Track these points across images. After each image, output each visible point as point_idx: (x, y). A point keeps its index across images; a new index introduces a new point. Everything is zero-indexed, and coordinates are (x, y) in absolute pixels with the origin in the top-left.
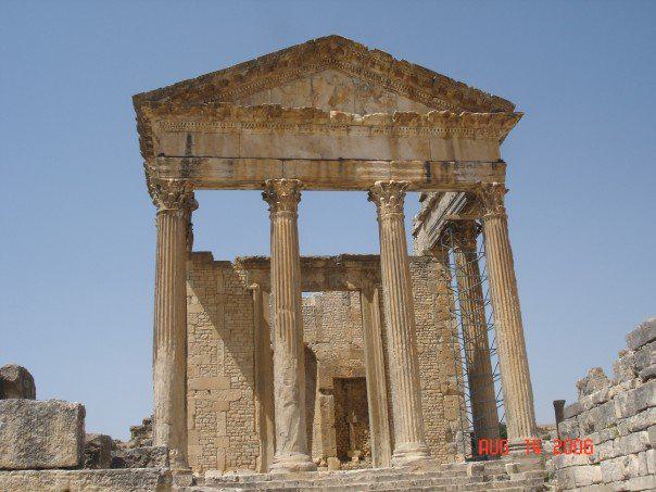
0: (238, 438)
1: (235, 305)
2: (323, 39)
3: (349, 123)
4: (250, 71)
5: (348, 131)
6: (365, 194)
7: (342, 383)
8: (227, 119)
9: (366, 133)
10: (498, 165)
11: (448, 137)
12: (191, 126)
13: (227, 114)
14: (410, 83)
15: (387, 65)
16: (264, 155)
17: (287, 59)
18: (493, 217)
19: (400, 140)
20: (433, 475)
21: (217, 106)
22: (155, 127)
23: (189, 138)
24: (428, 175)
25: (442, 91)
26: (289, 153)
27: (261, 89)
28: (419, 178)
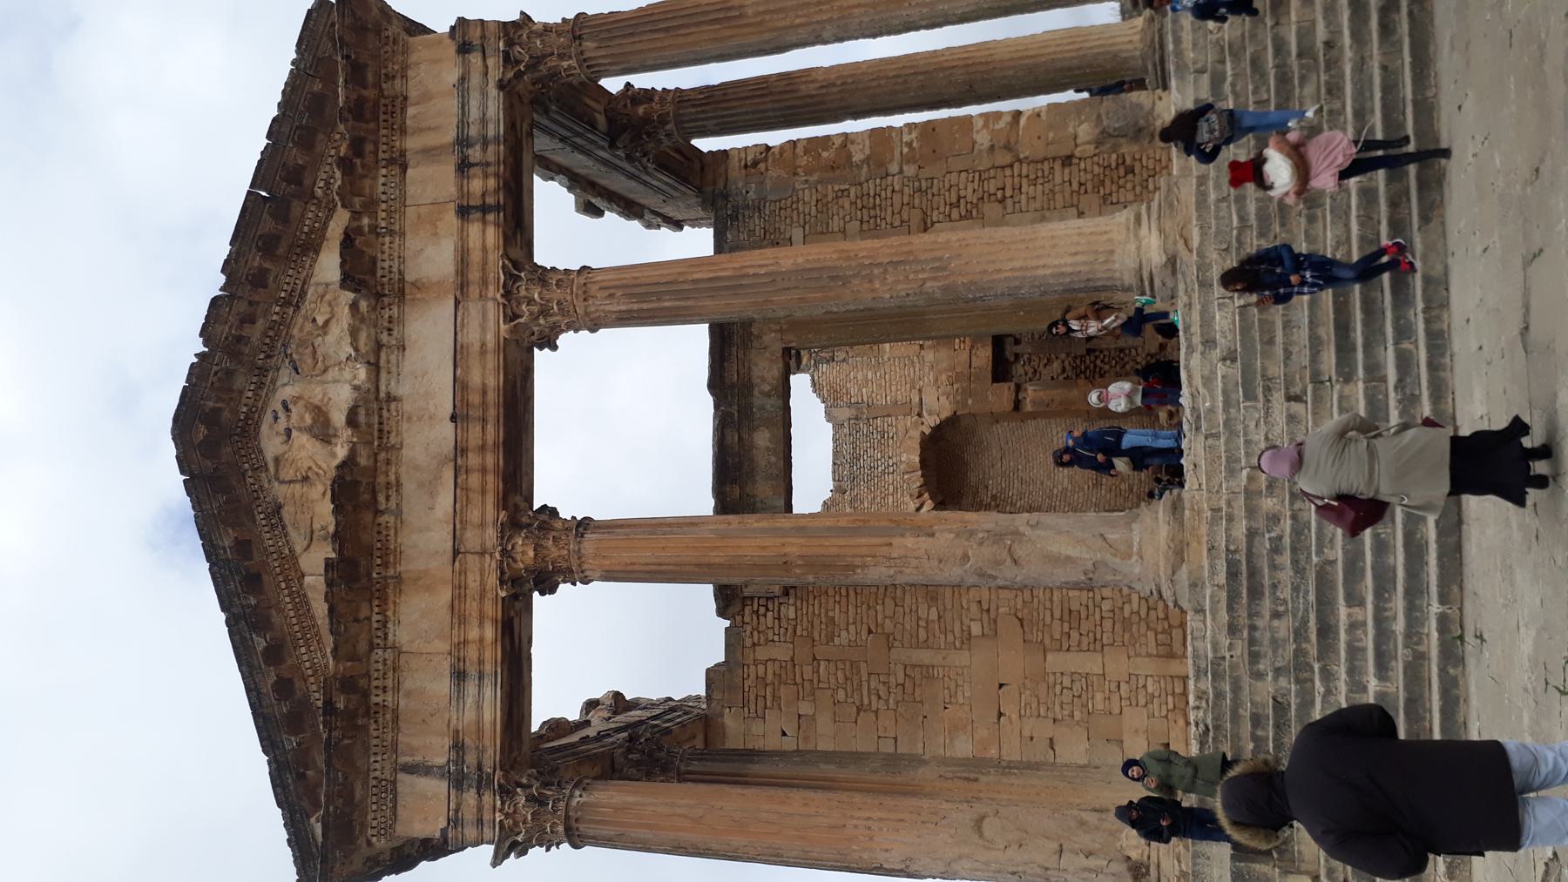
0: (1108, 624)
1: (816, 621)
3: (372, 397)
5: (391, 398)
7: (1001, 370)
8: (363, 682)
10: (466, 35)
14: (281, 251)
16: (446, 595)
17: (226, 544)
20: (1201, 202)
22: (380, 844)
23: (411, 769)
24: (484, 209)
25: (295, 176)
27: (301, 601)
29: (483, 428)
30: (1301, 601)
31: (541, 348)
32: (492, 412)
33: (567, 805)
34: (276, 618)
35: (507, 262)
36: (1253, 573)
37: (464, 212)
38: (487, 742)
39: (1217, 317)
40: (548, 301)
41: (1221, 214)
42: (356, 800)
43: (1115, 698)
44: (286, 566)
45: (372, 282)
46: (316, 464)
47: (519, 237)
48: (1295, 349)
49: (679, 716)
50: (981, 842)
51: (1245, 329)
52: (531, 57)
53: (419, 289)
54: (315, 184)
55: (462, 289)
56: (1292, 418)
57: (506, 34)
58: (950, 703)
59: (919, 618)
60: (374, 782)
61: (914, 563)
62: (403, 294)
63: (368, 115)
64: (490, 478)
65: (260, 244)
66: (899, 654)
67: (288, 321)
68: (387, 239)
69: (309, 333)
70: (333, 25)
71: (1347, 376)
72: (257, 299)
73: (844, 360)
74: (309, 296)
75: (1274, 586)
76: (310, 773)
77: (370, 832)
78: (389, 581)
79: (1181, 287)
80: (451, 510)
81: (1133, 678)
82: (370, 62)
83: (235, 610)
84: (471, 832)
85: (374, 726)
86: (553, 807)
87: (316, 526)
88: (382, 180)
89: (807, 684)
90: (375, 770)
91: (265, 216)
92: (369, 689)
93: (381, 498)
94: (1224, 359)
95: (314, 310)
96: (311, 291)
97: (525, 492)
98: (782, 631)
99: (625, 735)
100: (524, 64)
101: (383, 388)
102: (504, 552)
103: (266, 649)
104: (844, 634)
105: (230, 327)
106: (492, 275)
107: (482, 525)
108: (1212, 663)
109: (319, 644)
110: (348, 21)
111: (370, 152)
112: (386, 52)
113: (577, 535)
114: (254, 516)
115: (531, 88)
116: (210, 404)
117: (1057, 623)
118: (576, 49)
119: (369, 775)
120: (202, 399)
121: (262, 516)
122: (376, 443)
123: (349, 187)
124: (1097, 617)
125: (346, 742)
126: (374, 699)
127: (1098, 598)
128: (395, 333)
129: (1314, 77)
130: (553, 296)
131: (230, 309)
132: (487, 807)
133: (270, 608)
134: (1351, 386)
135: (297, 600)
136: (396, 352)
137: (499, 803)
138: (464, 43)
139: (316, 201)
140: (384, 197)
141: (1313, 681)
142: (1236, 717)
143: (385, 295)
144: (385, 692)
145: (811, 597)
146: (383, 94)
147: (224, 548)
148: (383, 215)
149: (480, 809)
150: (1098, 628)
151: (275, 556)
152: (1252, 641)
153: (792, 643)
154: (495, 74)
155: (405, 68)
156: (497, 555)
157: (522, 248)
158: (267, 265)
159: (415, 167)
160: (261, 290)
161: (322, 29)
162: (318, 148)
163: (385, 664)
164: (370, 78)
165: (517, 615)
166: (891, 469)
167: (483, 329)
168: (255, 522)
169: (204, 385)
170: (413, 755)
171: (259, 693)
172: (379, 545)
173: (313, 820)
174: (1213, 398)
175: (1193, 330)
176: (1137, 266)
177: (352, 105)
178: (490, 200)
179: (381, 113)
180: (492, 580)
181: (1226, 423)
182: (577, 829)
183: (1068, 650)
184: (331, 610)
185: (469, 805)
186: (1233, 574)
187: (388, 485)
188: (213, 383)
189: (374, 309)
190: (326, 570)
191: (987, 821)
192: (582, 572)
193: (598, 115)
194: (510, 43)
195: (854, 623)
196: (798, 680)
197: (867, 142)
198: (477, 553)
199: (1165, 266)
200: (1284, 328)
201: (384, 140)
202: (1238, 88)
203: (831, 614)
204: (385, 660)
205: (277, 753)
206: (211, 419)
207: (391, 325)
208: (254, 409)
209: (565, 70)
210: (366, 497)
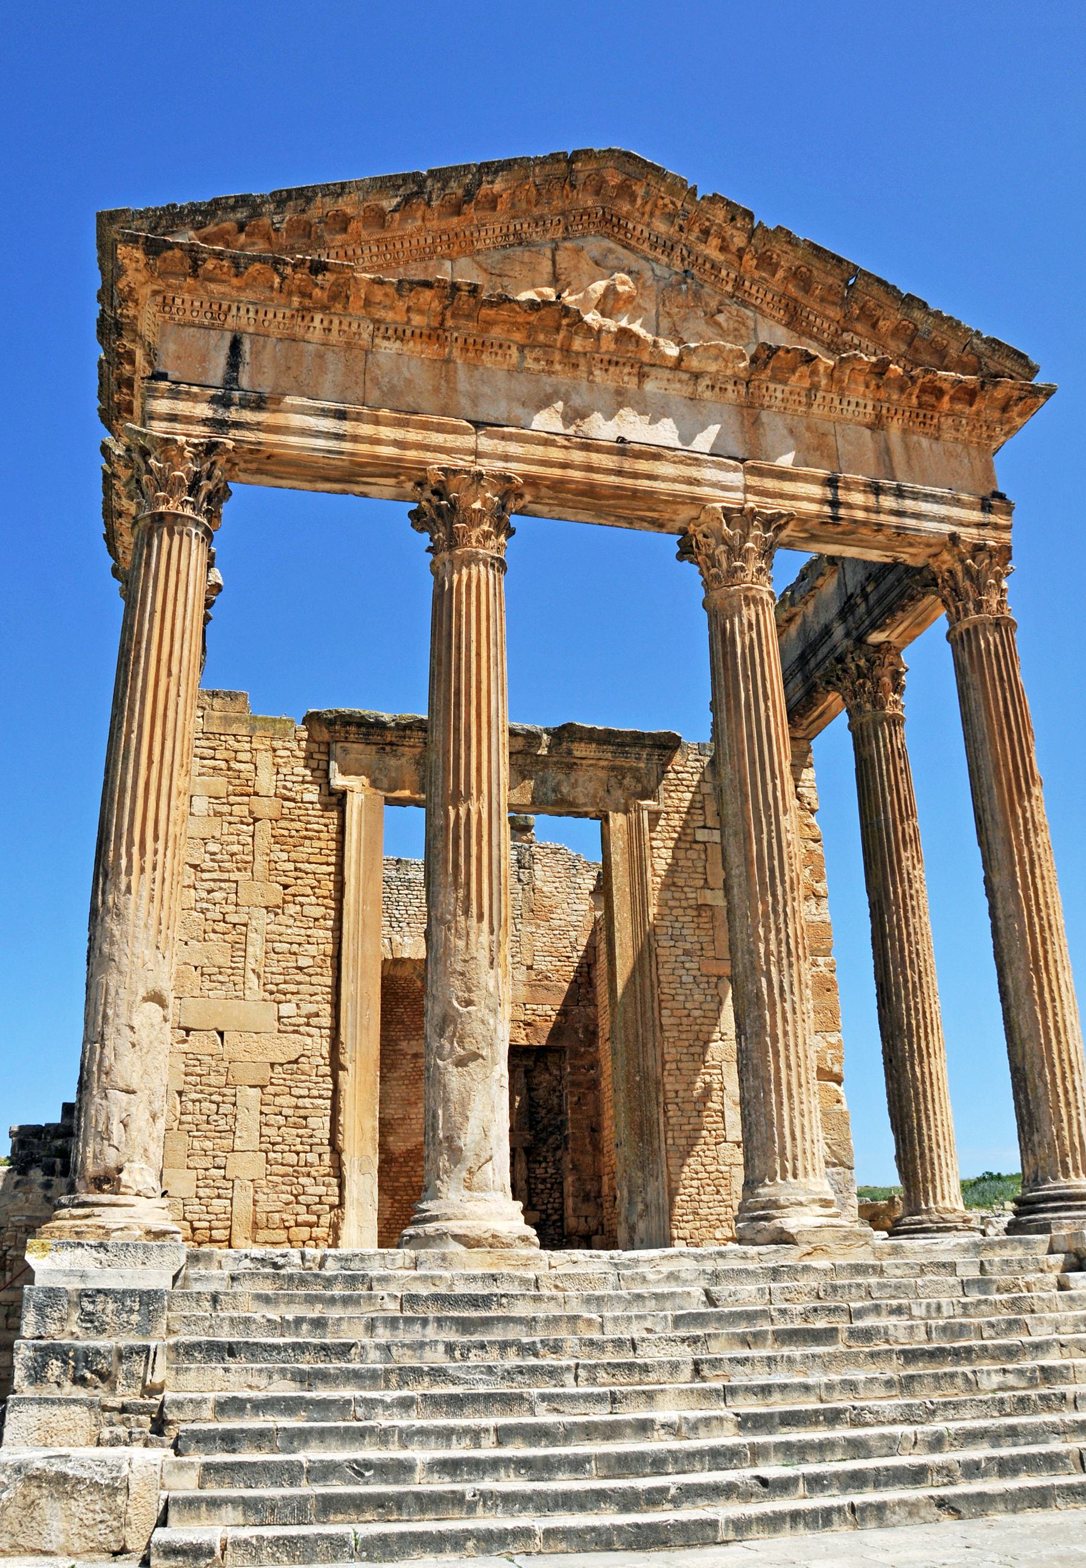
0: (292, 1158)
1: (298, 825)
2: (587, 154)
3: (646, 358)
4: (407, 200)
5: (642, 376)
6: (671, 543)
8: (338, 307)
12: (243, 320)
14: (792, 289)
15: (739, 240)
17: (498, 187)
19: (765, 416)
20: (859, 1269)
21: (318, 268)
23: (235, 346)
24: (835, 504)
27: (426, 255)
28: (814, 508)
30: (477, 1377)
31: (679, 542)
32: (628, 482)
34: (410, 227)
36: (487, 1322)
37: (831, 483)
39: (749, 1288)
41: (853, 1290)
43: (207, 1162)
45: (763, 377)
47: (802, 535)
48: (747, 1369)
50: (139, 998)
51: (750, 1317)
52: (978, 571)
54: (856, 333)
56: (675, 1367)
58: (202, 974)
59: (300, 944)
60: (225, 307)
61: (461, 944)
63: (925, 398)
64: (557, 472)
65: (803, 269)
66: (261, 920)
68: (804, 400)
69: (707, 305)
70: (1011, 377)
71: (747, 1423)
72: (746, 257)
73: (520, 880)
75: (482, 1346)
79: (763, 1249)
81: (229, 1184)
82: (974, 408)
83: (429, 182)
85: (288, 313)
86: (187, 502)
87: (506, 281)
89: (226, 809)
90: (238, 309)
91: (830, 280)
93: (538, 352)
94: (707, 1293)
98: (289, 785)
101: (653, 372)
103: (382, 209)
104: (284, 856)
106: (769, 500)
108: (363, 1276)
110: (1016, 394)
117: (293, 1101)
121: (518, 227)
122: (597, 356)
124: (299, 1148)
127: (320, 1149)
128: (708, 394)
129: (1023, 1384)
130: (752, 563)
132: (191, 427)
133: (423, 219)
134: (734, 1430)
136: (690, 389)
137: (196, 441)
138: (990, 506)
140: (845, 403)
141: (387, 1387)
142: (311, 1300)
145: (327, 821)
147: (492, 182)
148: (828, 400)
149: (188, 420)
150: (287, 1148)
151: (476, 235)
152: (409, 1321)
153: (276, 795)
155: (966, 444)
160: (755, 262)
162: (892, 344)
164: (959, 407)
166: (394, 924)
167: (714, 485)
168: (513, 218)
171: (339, 195)
172: (488, 344)
173: (192, 233)
174: (659, 1281)
175: (720, 1261)
176: (782, 1202)
177: (937, 383)
178: (842, 512)
181: (639, 1297)
183: (262, 1113)
186: (484, 1301)
187: (550, 362)
189: (735, 375)
190: (470, 284)
191: (155, 1006)
195: (296, 869)
196: (232, 799)
197: (817, 918)
199: (782, 1231)
200: (769, 1358)
202: (983, 1307)
203: (307, 842)
206: (625, 190)
207: (717, 389)
210: (541, 337)
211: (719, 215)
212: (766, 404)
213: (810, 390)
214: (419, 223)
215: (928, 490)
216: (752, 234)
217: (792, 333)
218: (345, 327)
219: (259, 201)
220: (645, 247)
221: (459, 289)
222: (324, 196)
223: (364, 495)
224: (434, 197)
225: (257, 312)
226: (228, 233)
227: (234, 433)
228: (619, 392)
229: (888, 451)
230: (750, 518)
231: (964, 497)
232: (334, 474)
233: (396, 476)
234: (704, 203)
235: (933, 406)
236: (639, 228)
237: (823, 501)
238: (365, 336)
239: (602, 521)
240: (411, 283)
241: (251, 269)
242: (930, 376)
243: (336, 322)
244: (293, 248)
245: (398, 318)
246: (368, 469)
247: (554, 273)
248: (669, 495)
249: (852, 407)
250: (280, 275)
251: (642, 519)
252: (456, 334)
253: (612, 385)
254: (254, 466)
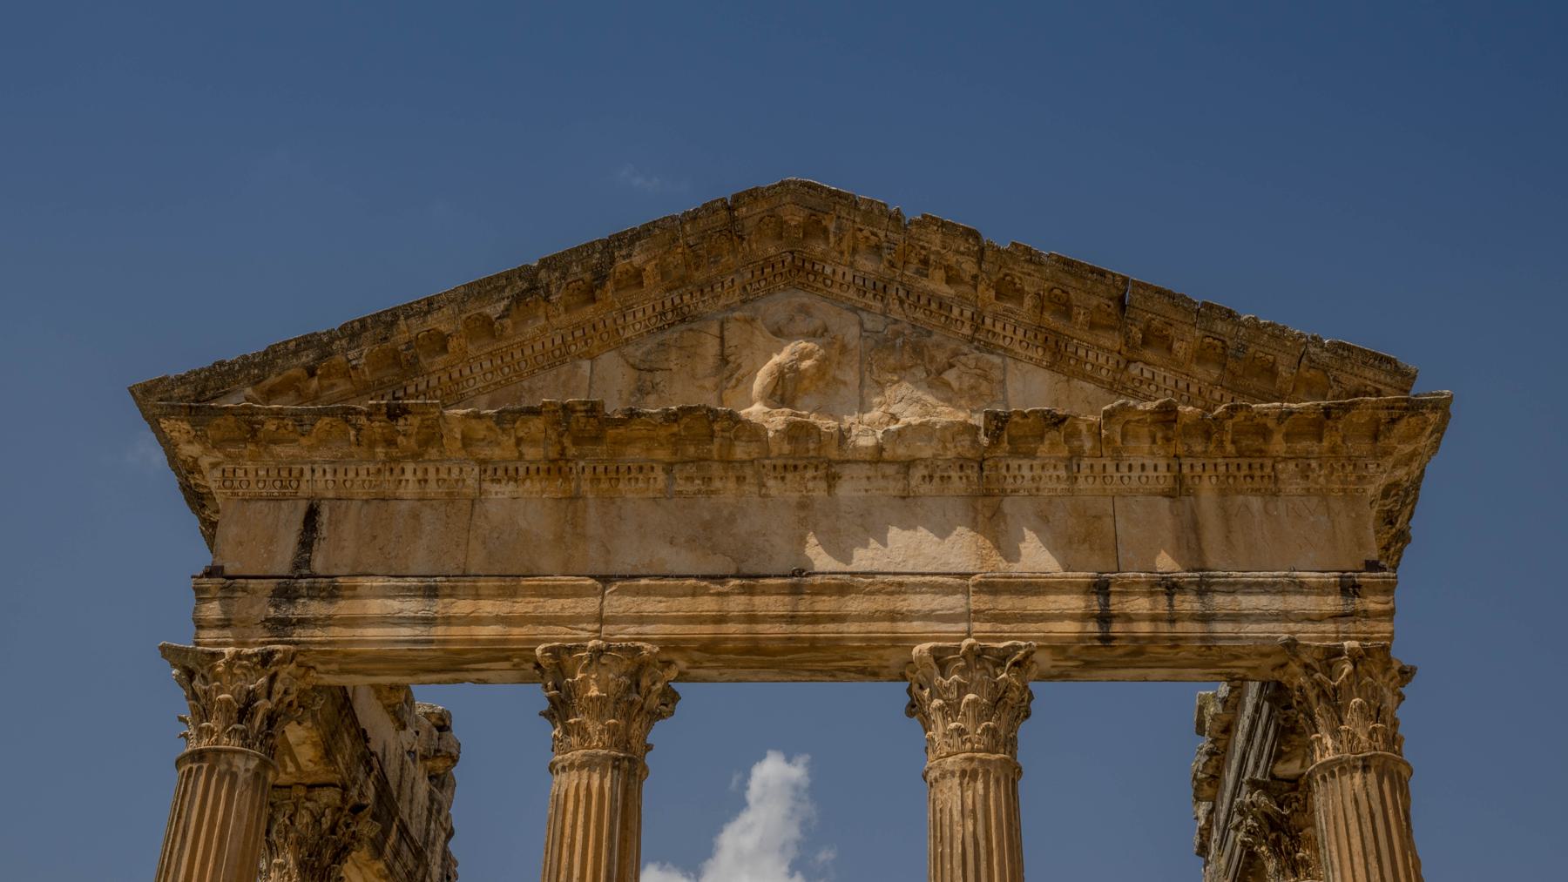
2: (753, 195)
3: (833, 454)
5: (832, 480)
8: (433, 452)
9: (895, 487)
11: (1179, 490)
12: (320, 483)
13: (432, 437)
14: (1050, 319)
15: (968, 267)
17: (637, 260)
18: (1343, 767)
19: (1008, 505)
21: (395, 413)
23: (312, 515)
24: (1105, 618)
25: (1156, 338)
26: (626, 560)
27: (558, 358)
28: (1069, 628)
29: (783, 616)
31: (909, 691)
32: (805, 630)
33: (235, 752)
34: (530, 329)
35: (1022, 652)
37: (1101, 588)
38: (338, 633)
40: (965, 714)
42: (272, 446)
44: (605, 336)
45: (999, 453)
46: (743, 376)
49: (405, 866)
52: (1335, 689)
53: (990, 519)
55: (987, 584)
57: (1367, 650)
62: (985, 496)
63: (1244, 443)
64: (706, 631)
65: (1057, 292)
67: (953, 328)
68: (1063, 473)
69: (932, 359)
70: (1378, 393)
72: (981, 288)
74: (986, 356)
76: (315, 383)
77: (229, 467)
78: (573, 484)
80: (668, 569)
82: (1325, 443)
83: (543, 274)
84: (213, 610)
85: (373, 470)
87: (658, 376)
88: (1149, 463)
90: (313, 471)
91: (1094, 301)
92: (424, 461)
93: (691, 469)
95: (965, 365)
96: (996, 360)
97: (694, 672)
99: (371, 793)
100: (1324, 678)
101: (847, 471)
102: (599, 652)
103: (488, 317)
105: (938, 253)
106: (1005, 627)
107: (641, 620)
109: (496, 383)
110: (1383, 415)
111: (1189, 447)
112: (1343, 466)
113: (616, 759)
114: (676, 288)
115: (1296, 683)
116: (832, 227)
118: (1348, 761)
119: (306, 463)
120: (839, 217)
121: (677, 301)
122: (767, 462)
123: (1137, 418)
125: (353, 432)
126: (410, 467)
128: (925, 488)
131: (963, 254)
133: (547, 318)
135: (557, 353)
136: (900, 485)
138: (1356, 586)
139: (1122, 366)
140: (1124, 469)
143: (981, 469)
144: (419, 481)
146: (1279, 462)
147: (629, 256)
148: (1098, 468)
154: (1308, 634)
155: (1324, 495)
156: (590, 644)
157: (1053, 667)
158: (1028, 302)
159: (1172, 512)
160: (993, 293)
161: (1370, 375)
162: (1198, 370)
163: (457, 481)
164: (1302, 445)
165: (514, 665)
167: (928, 616)
168: (669, 290)
169: (857, 219)
170: (330, 524)
171: (429, 312)
172: (622, 470)
173: (249, 391)
177: (1258, 420)
178: (1117, 628)
179: (1248, 460)
180: (562, 634)
182: (200, 768)
184: (533, 412)
185: (252, 607)
188: (861, 230)
189: (960, 457)
190: (585, 403)
192: (564, 768)
193: (1298, 763)
194: (1357, 658)
198: (602, 610)
201: (1209, 467)
204: (464, 480)
205: (343, 342)
206: (814, 228)
207: (936, 480)
208: (829, 282)
209: (1320, 740)
210: (691, 450)
211: (935, 240)
212: (1009, 487)
213: (1070, 459)
214: (542, 322)
215: (1252, 576)
216: (980, 256)
217: (1057, 377)
218: (443, 475)
219: (325, 339)
220: (852, 294)
221: (574, 411)
222: (407, 318)
223: (485, 682)
224: (554, 291)
225: (335, 471)
226: (298, 379)
227: (300, 634)
228: (803, 505)
229: (1196, 527)
230: (971, 658)
231: (1311, 577)
232: (433, 665)
233: (507, 659)
234: (914, 229)
235: (1261, 451)
236: (840, 271)
237: (1084, 618)
238: (469, 482)
239: (793, 677)
240: (514, 412)
241: (318, 425)
242: (1240, 416)
243: (432, 470)
244: (382, 383)
245: (507, 455)
246: (470, 656)
247: (722, 354)
248: (861, 639)
249: (1135, 474)
250: (354, 426)
251: (845, 670)
252: (582, 463)
253: (795, 496)
254: (334, 667)
